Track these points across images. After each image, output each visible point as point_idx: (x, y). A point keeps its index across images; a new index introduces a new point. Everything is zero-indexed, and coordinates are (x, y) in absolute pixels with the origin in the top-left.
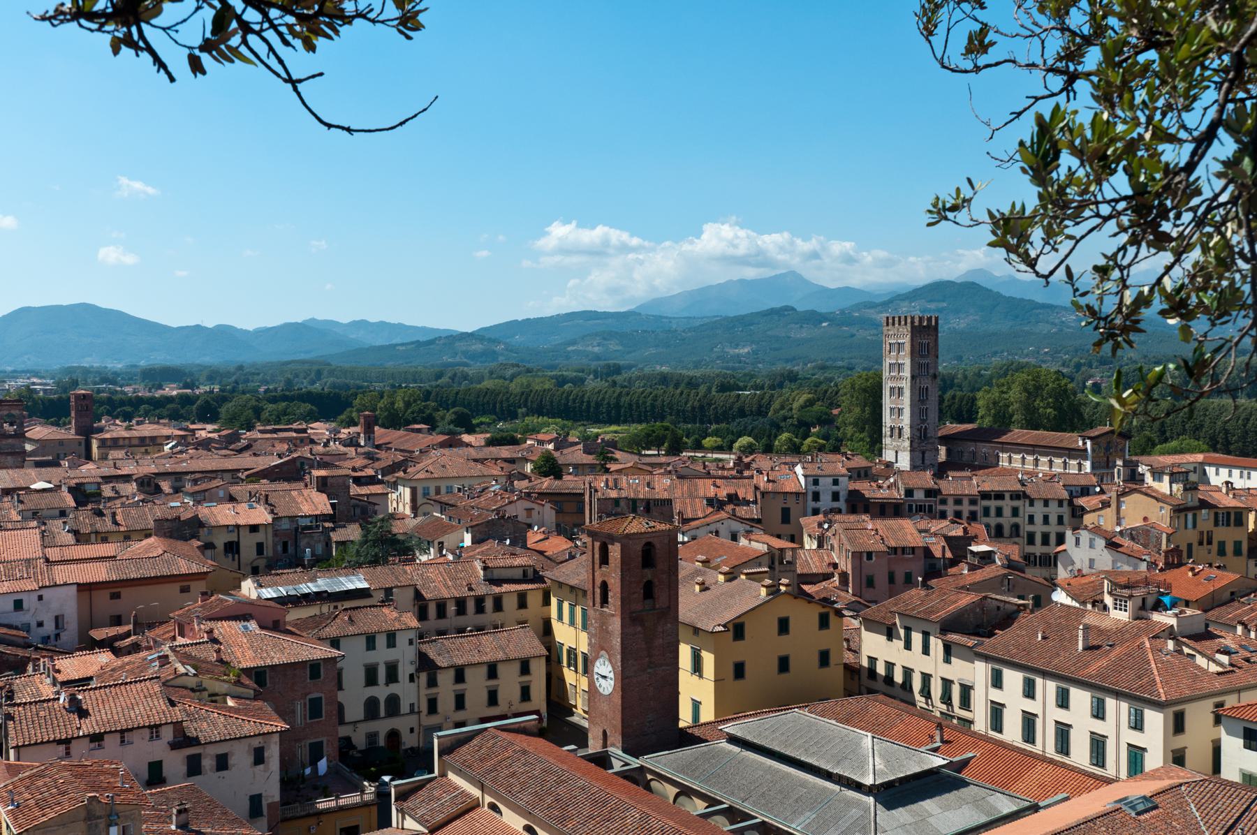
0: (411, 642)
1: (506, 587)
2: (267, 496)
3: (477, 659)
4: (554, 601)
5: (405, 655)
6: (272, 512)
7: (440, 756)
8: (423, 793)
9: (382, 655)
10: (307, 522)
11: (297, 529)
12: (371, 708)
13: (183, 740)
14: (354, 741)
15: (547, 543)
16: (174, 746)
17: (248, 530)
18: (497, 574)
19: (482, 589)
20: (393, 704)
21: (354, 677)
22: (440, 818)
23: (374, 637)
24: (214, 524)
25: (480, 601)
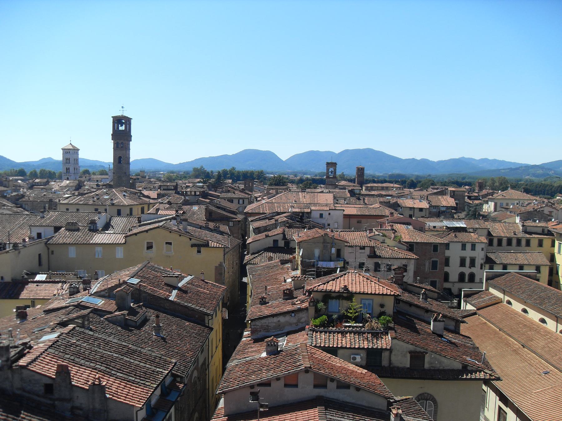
0: (482, 249)
1: (534, 236)
2: (427, 197)
3: (514, 262)
4: (557, 243)
5: (479, 255)
6: (429, 203)
7: (486, 280)
8: (476, 296)
9: (468, 253)
10: (444, 209)
11: (439, 212)
12: (462, 277)
13: (373, 255)
14: (453, 291)
15: (558, 226)
16: (369, 257)
17: (418, 210)
18: (529, 229)
19: (521, 235)
20: (472, 278)
21: (455, 262)
22: (483, 304)
23: (465, 244)
24: (403, 205)
25: (519, 241)
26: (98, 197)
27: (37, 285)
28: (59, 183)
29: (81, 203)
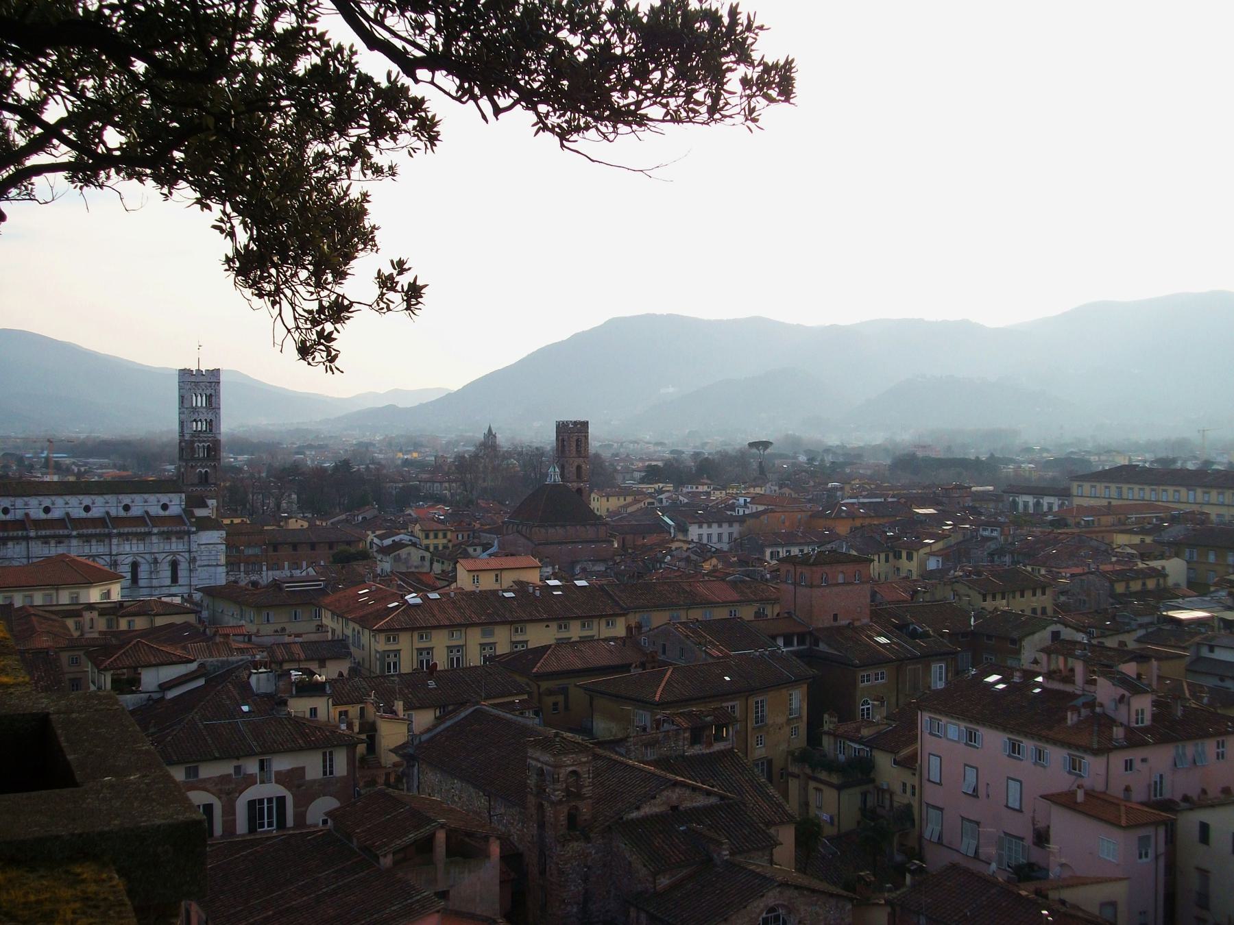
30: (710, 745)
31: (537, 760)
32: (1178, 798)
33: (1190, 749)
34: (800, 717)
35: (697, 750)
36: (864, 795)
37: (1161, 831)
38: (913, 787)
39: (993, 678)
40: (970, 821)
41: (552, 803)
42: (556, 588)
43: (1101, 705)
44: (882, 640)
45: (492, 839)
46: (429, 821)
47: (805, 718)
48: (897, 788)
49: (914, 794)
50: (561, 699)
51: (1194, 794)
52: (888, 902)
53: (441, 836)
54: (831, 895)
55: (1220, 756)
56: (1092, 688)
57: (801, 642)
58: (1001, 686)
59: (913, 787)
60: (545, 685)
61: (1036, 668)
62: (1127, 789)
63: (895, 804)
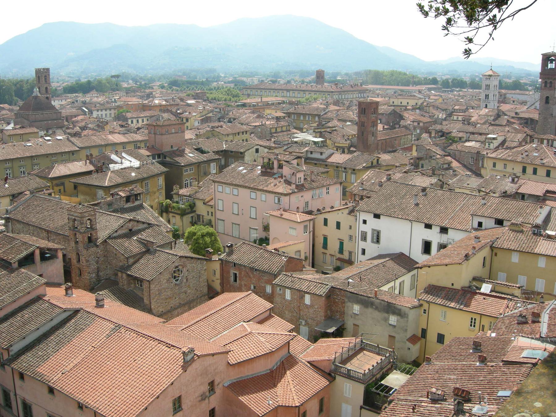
26: (527, 153)
27: (484, 299)
28: (478, 111)
29: (510, 158)
30: (133, 202)
31: (72, 215)
32: (315, 210)
33: (317, 191)
34: (162, 188)
35: (129, 205)
36: (192, 217)
37: (312, 222)
38: (212, 213)
39: (241, 168)
40: (236, 224)
41: (81, 233)
42: (49, 140)
43: (285, 177)
44: (191, 155)
45: (59, 251)
46: (31, 246)
47: (164, 188)
48: (205, 214)
49: (212, 215)
50: (62, 188)
51: (321, 208)
52: (219, 259)
53: (37, 252)
54: (199, 259)
55: (328, 193)
56: (280, 170)
57: (159, 157)
58: (245, 171)
59: (212, 213)
60: (55, 182)
61: (256, 163)
62: (298, 208)
63: (205, 220)
